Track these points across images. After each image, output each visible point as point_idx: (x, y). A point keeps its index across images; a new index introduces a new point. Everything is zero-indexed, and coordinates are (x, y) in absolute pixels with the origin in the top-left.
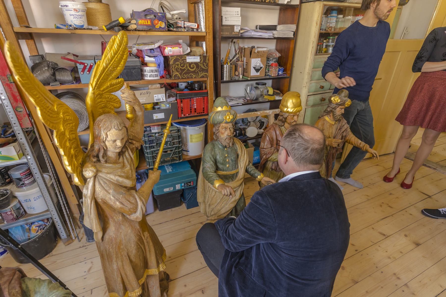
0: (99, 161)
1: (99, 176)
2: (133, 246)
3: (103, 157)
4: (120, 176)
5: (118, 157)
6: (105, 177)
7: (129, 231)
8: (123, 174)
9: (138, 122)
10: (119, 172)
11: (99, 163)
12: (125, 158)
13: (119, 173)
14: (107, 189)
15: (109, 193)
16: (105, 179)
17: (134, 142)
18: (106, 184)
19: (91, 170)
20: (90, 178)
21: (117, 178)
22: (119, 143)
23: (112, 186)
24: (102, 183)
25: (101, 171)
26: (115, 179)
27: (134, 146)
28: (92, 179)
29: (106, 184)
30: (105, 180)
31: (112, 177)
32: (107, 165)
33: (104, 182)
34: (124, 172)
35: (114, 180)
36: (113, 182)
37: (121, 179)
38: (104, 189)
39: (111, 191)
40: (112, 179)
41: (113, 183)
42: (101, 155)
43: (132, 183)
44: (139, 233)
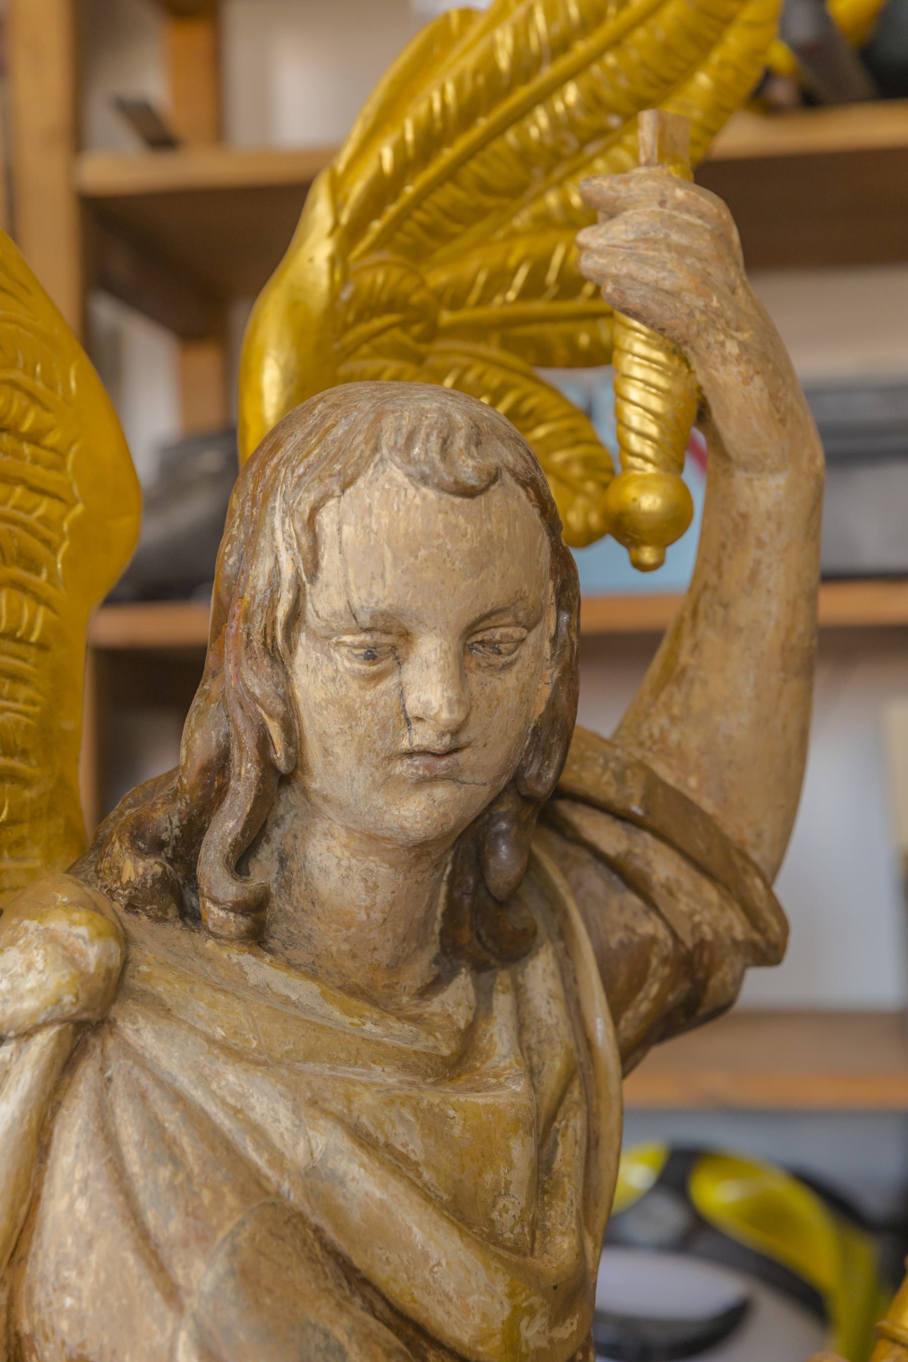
0: (176, 896)
1: (127, 1050)
3: (240, 860)
4: (362, 1138)
5: (421, 968)
6: (186, 1082)
8: (412, 1142)
9: (745, 611)
10: (373, 1088)
11: (174, 931)
12: (502, 1003)
14: (168, 1225)
15: (173, 1294)
16: (179, 1099)
17: (663, 867)
18: (177, 1162)
19: (52, 939)
20: (26, 1035)
21: (325, 1141)
22: (428, 686)
23: (231, 1216)
24: (129, 1131)
25: (162, 1010)
26: (298, 1155)
27: (649, 926)
28: (42, 1044)
29: (177, 1162)
30: (171, 1120)
31: (269, 1105)
32: (259, 970)
33: (154, 1129)
34: (433, 1123)
35: (278, 1160)
37: (363, 1184)
38: (133, 1214)
39: (202, 1274)
40: (256, 1131)
41: (251, 1185)
42: (226, 826)
43: (502, 1312)
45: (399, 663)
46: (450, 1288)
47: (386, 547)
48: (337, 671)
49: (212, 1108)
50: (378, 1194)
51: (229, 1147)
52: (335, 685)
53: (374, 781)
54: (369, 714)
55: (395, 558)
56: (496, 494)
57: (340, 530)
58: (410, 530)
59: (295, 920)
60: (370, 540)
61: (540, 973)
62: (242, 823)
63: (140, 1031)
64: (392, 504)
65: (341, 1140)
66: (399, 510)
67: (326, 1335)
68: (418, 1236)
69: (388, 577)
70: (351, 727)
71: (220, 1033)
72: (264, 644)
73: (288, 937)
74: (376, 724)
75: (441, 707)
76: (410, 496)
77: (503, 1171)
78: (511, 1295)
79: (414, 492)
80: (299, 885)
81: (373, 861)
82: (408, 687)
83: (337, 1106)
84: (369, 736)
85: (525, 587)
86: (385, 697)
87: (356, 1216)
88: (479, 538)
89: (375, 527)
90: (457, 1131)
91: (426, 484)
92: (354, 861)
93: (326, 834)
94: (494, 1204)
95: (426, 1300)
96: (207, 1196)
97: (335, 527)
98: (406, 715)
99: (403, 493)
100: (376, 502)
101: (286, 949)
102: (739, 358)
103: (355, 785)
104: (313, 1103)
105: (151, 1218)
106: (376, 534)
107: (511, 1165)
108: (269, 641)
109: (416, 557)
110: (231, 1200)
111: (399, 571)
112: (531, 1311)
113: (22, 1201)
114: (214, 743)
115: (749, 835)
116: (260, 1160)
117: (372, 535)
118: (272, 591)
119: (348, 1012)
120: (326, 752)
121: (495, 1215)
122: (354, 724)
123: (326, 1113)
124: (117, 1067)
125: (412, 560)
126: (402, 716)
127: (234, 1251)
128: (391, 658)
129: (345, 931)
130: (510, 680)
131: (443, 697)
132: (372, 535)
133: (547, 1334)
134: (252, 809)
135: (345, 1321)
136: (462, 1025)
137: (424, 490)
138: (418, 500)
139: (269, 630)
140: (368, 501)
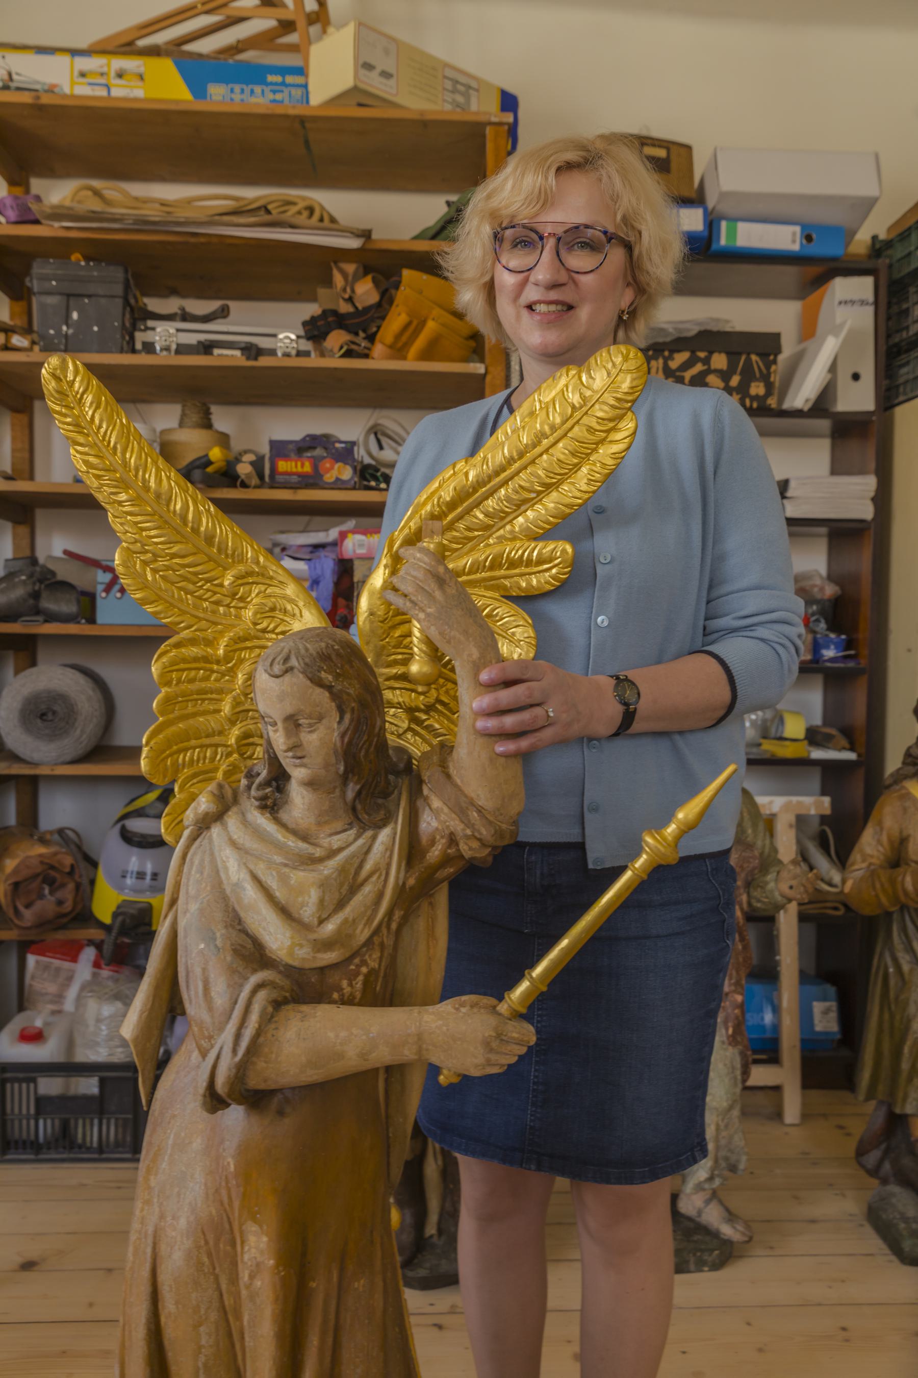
2: (183, 1223)
4: (255, 878)
7: (197, 1143)
8: (272, 883)
13: (260, 869)
16: (212, 854)
18: (202, 873)
21: (244, 876)
29: (202, 873)
30: (207, 859)
33: (202, 861)
34: (284, 880)
35: (228, 878)
36: (220, 883)
37: (251, 893)
43: (288, 943)
44: (224, 1193)
46: (272, 931)
49: (218, 859)
50: (254, 896)
51: (217, 872)
56: (287, 678)
61: (384, 835)
63: (216, 831)
65: (248, 877)
67: (214, 934)
68: (264, 911)
71: (235, 837)
77: (306, 898)
78: (292, 938)
83: (252, 867)
85: (302, 707)
87: (246, 901)
90: (292, 882)
94: (301, 908)
95: (263, 932)
96: (204, 885)
102: (424, 620)
104: (245, 864)
105: (190, 888)
107: (310, 897)
110: (209, 888)
112: (301, 946)
113: (178, 875)
115: (473, 795)
116: (223, 876)
119: (284, 837)
121: (301, 912)
123: (247, 867)
124: (206, 841)
127: (202, 903)
130: (314, 736)
133: (312, 954)
135: (224, 931)
136: (335, 847)
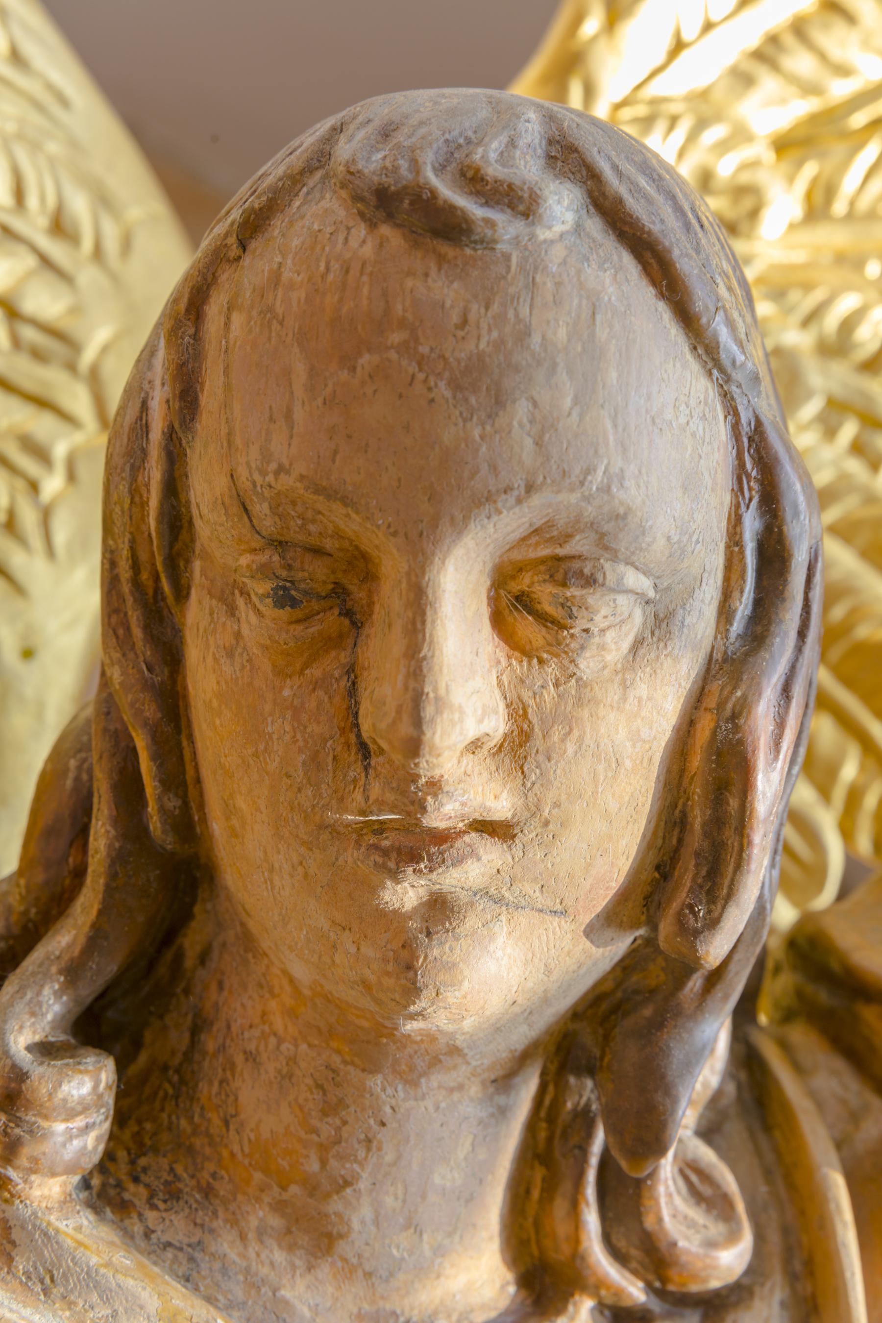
45: (353, 623)
47: (296, 350)
48: (238, 635)
52: (232, 665)
53: (306, 875)
54: (288, 728)
55: (312, 372)
57: (227, 325)
58: (344, 310)
59: (190, 1150)
60: (269, 339)
62: (82, 940)
64: (318, 260)
66: (328, 269)
69: (299, 414)
70: (256, 755)
72: (136, 582)
73: (167, 1183)
74: (300, 751)
75: (399, 711)
76: (354, 243)
79: (363, 233)
80: (210, 1083)
81: (339, 1052)
82: (365, 674)
84: (289, 776)
86: (320, 693)
88: (495, 334)
89: (280, 309)
91: (390, 217)
92: (304, 1047)
93: (260, 985)
97: (223, 320)
98: (359, 735)
99: (341, 238)
100: (289, 261)
101: (154, 1207)
103: (276, 879)
106: (281, 323)
108: (145, 576)
109: (354, 369)
111: (320, 400)
114: (69, 783)
117: (275, 325)
118: (132, 466)
120: (230, 811)
122: (262, 747)
125: (344, 375)
126: (353, 738)
128: (336, 611)
129: (276, 1189)
131: (406, 688)
132: (275, 325)
134: (100, 913)
137: (385, 230)
138: (368, 251)
139: (143, 557)
140: (278, 259)
